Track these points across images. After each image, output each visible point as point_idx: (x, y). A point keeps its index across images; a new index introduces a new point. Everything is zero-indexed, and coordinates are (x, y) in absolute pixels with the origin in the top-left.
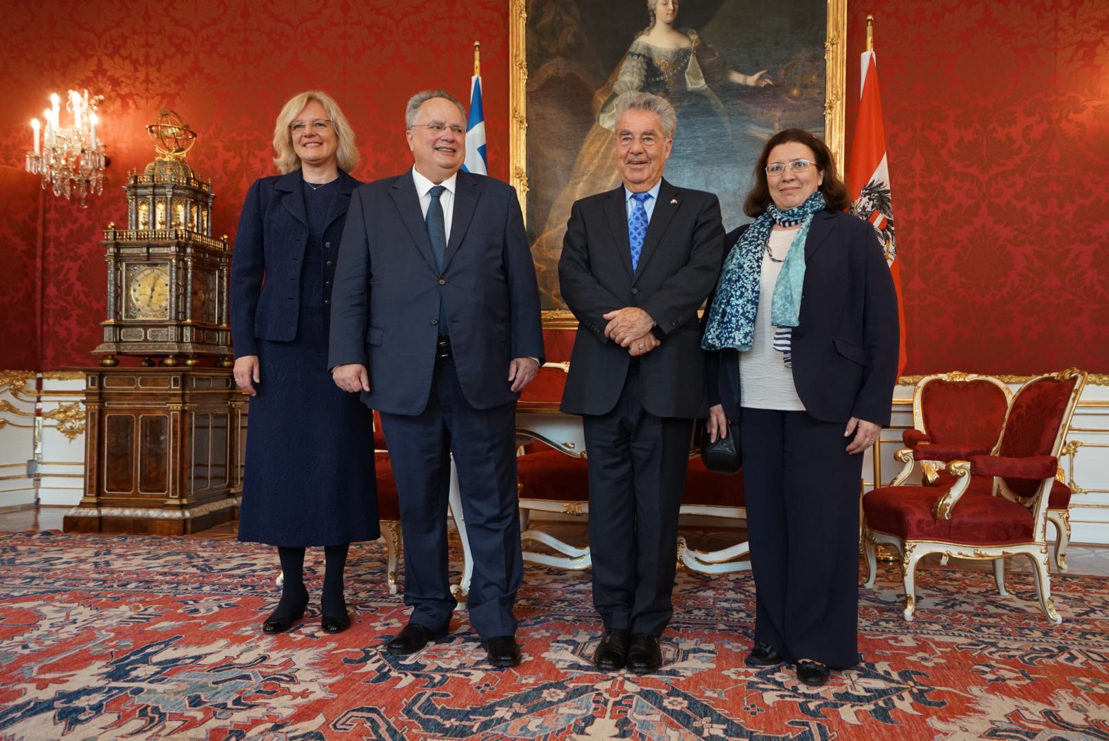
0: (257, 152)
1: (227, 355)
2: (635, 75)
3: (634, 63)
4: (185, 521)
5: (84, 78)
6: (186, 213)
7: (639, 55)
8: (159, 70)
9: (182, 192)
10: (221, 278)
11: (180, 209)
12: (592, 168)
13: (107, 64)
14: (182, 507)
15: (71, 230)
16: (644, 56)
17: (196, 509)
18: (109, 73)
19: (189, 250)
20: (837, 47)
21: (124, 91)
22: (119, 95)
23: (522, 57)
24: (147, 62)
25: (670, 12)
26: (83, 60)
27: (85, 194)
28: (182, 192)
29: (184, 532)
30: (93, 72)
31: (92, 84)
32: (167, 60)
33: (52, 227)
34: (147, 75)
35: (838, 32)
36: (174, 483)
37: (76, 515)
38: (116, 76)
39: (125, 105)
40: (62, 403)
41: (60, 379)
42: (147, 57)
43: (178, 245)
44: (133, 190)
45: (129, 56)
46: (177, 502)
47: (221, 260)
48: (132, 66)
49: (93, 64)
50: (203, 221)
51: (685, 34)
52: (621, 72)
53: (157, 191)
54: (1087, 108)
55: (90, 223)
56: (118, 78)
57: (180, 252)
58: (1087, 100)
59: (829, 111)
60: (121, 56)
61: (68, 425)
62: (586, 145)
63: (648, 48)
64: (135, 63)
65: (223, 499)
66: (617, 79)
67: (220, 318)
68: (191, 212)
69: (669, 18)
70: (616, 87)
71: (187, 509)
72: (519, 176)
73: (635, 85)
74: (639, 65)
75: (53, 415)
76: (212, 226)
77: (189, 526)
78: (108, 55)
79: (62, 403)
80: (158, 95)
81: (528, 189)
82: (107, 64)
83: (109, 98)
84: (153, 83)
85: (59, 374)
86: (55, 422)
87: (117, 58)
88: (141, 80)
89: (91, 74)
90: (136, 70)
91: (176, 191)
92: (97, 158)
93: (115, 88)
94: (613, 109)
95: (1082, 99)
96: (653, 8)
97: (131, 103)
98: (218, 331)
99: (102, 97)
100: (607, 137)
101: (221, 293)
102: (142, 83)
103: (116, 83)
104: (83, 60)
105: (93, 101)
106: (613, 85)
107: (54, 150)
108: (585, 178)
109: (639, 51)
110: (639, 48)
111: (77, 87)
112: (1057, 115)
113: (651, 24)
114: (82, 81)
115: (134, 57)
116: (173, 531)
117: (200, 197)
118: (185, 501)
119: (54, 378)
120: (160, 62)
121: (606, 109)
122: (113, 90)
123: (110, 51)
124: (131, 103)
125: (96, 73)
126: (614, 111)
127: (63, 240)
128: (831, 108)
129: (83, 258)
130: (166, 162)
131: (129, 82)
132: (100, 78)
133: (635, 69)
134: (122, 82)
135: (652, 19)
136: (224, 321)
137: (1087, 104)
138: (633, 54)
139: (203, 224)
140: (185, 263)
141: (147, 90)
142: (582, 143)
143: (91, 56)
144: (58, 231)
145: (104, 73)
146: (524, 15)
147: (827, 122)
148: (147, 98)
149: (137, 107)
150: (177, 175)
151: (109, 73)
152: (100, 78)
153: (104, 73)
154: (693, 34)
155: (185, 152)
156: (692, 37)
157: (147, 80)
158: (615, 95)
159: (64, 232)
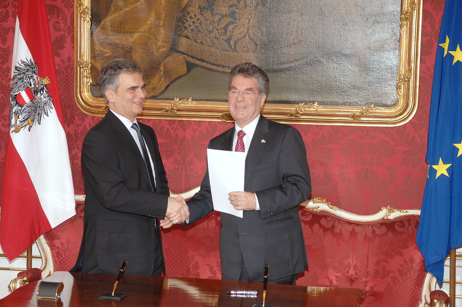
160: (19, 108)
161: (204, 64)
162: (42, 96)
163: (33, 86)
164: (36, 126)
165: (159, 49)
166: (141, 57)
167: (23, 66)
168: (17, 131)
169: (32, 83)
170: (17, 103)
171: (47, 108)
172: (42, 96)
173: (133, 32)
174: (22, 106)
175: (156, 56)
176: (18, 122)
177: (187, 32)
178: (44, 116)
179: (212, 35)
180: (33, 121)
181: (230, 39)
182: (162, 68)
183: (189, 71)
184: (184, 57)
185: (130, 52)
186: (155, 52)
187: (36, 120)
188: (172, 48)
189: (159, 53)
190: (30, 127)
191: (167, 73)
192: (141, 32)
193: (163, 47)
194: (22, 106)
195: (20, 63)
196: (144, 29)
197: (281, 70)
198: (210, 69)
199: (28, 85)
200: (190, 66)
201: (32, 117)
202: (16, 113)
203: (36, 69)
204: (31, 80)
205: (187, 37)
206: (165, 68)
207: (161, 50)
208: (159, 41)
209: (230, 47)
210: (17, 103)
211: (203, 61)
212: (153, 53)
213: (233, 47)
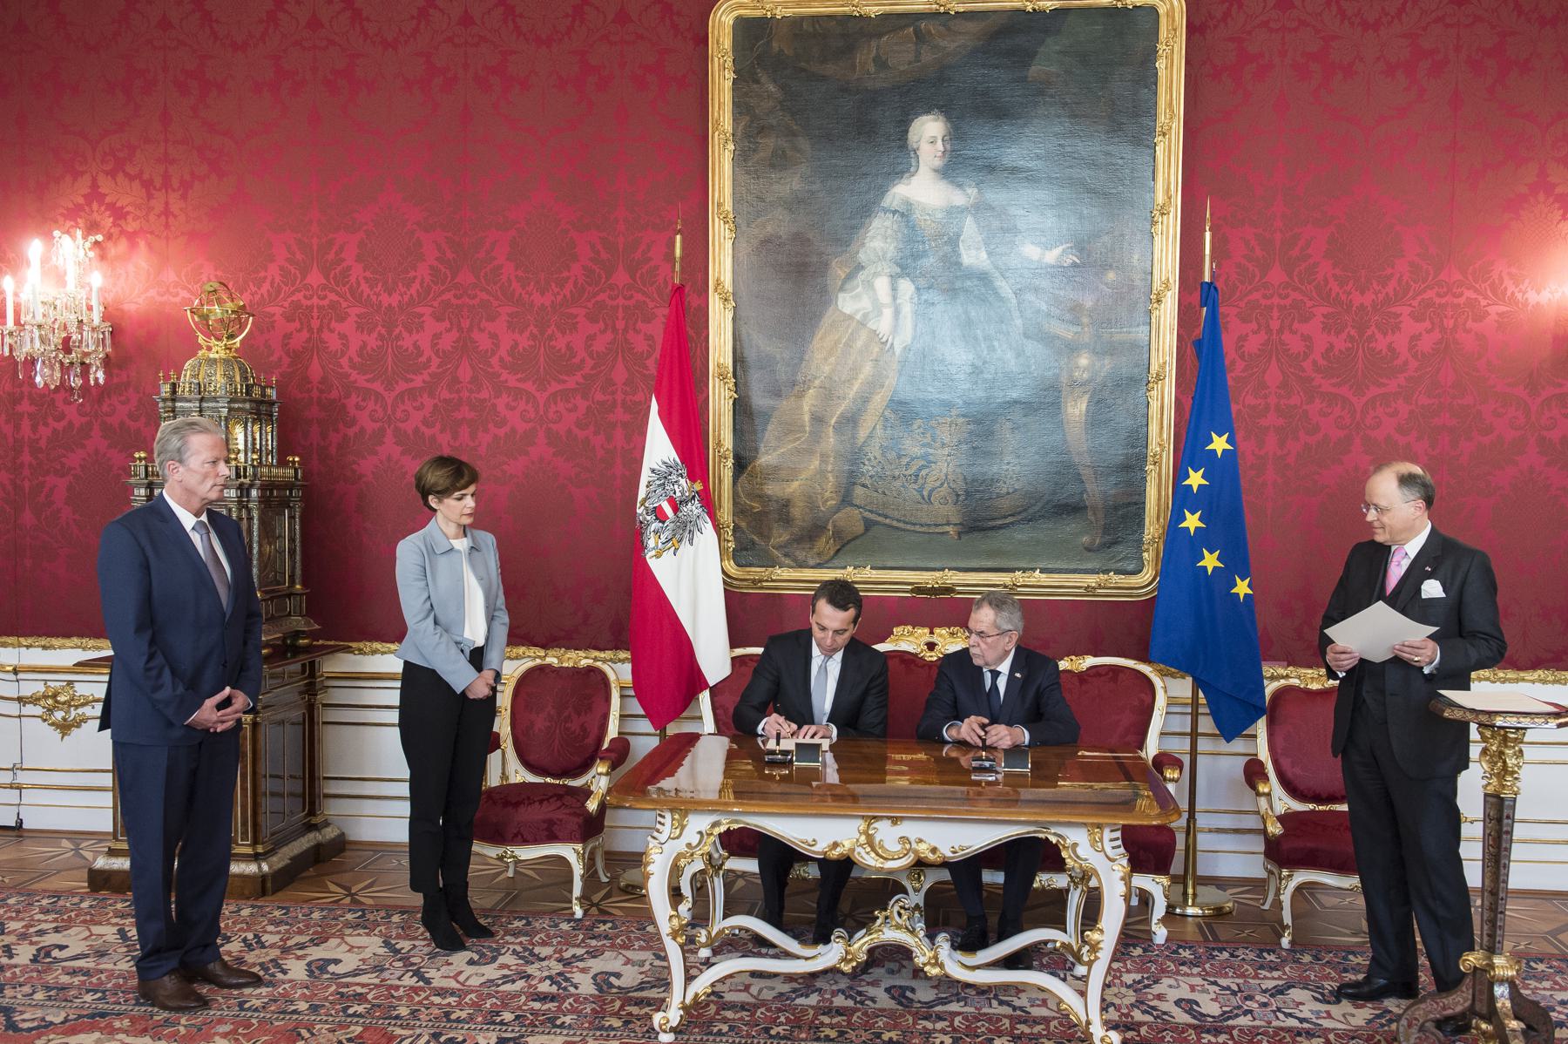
0: (333, 324)
1: (303, 632)
2: (889, 240)
3: (888, 223)
4: (264, 877)
5: (71, 205)
6: (246, 436)
7: (895, 212)
8: (184, 197)
9: (241, 405)
10: (292, 517)
11: (239, 433)
12: (827, 369)
13: (105, 185)
14: (256, 857)
15: (55, 431)
16: (903, 215)
17: (275, 859)
18: (108, 200)
19: (254, 493)
20: (1168, 218)
21: (131, 225)
22: (123, 232)
23: (728, 206)
24: (166, 185)
25: (940, 154)
26: (68, 178)
27: (79, 382)
28: (241, 405)
29: (264, 893)
30: (85, 196)
31: (82, 214)
32: (196, 183)
33: (26, 424)
34: (167, 204)
35: (1170, 198)
36: (244, 824)
37: (107, 867)
38: (119, 204)
39: (133, 245)
40: (49, 683)
41: (44, 647)
42: (166, 178)
43: (240, 487)
44: (169, 404)
45: (139, 176)
46: (249, 851)
47: (291, 493)
48: (144, 190)
49: (83, 185)
50: (267, 440)
51: (960, 186)
52: (869, 234)
53: (205, 405)
54: (1489, 314)
55: (84, 420)
56: (122, 208)
57: (242, 496)
58: (1489, 305)
59: (1155, 305)
60: (127, 175)
61: (59, 715)
62: (819, 334)
63: (908, 204)
64: (148, 185)
65: (303, 836)
66: (863, 244)
67: (292, 577)
68: (252, 432)
69: (938, 163)
70: (862, 257)
71: (264, 860)
72: (722, 377)
73: (889, 255)
74: (895, 227)
75: (39, 699)
76: (278, 445)
77: (269, 885)
78: (107, 173)
79: (49, 683)
80: (182, 233)
81: (736, 396)
82: (105, 185)
83: (109, 237)
84: (175, 216)
85: (44, 641)
86: (38, 710)
87: (120, 177)
88: (157, 211)
89: (81, 201)
90: (150, 196)
91: (232, 405)
92: (101, 336)
93: (120, 222)
94: (858, 286)
95: (1484, 302)
96: (915, 146)
97: (142, 244)
98: (289, 596)
99: (100, 238)
100: (848, 327)
101: (292, 540)
102: (159, 216)
103: (119, 214)
104: (68, 178)
105: (88, 245)
106: (858, 252)
107: (40, 326)
108: (817, 382)
109: (895, 205)
110: (895, 203)
111: (61, 219)
112: (1452, 322)
113: (912, 169)
114: (68, 209)
115: (146, 176)
116: (246, 892)
117: (263, 408)
118: (260, 849)
119: (38, 646)
120: (186, 186)
121: (847, 286)
122: (115, 224)
123: (109, 167)
124: (142, 244)
125: (89, 198)
126: (860, 289)
127: (43, 444)
128: (1159, 301)
129: (72, 472)
130: (215, 360)
131: (138, 212)
132: (95, 206)
133: (889, 232)
134: (128, 213)
135: (913, 162)
136: (297, 581)
137: (1488, 309)
138: (886, 211)
139: (267, 445)
140: (249, 511)
141: (167, 226)
142: (813, 334)
143: (82, 173)
144: (34, 428)
145: (101, 198)
146: (731, 147)
147: (1153, 320)
148: (167, 238)
149: (150, 246)
150: (231, 379)
151: (108, 200)
152: (95, 206)
153: (101, 198)
154: (970, 186)
155: (238, 339)
156: (969, 191)
157: (167, 212)
158: (860, 267)
159: (45, 432)
160: (661, 525)
161: (888, 521)
162: (694, 508)
163: (678, 494)
164: (685, 548)
165: (827, 501)
167: (664, 468)
168: (658, 556)
169: (677, 490)
170: (657, 519)
171: (700, 522)
172: (694, 508)
174: (663, 523)
176: (660, 544)
178: (697, 533)
179: (898, 484)
180: (680, 541)
181: (922, 488)
182: (830, 527)
183: (867, 529)
184: (861, 513)
185: (787, 506)
187: (686, 540)
188: (843, 501)
190: (676, 550)
191: (837, 534)
193: (833, 499)
194: (663, 523)
195: (660, 464)
197: (992, 528)
198: (897, 528)
199: (672, 494)
200: (869, 525)
201: (678, 536)
202: (656, 532)
203: (684, 472)
204: (676, 486)
205: (864, 486)
206: (835, 526)
209: (924, 499)
210: (657, 519)
211: (886, 517)
213: (926, 497)
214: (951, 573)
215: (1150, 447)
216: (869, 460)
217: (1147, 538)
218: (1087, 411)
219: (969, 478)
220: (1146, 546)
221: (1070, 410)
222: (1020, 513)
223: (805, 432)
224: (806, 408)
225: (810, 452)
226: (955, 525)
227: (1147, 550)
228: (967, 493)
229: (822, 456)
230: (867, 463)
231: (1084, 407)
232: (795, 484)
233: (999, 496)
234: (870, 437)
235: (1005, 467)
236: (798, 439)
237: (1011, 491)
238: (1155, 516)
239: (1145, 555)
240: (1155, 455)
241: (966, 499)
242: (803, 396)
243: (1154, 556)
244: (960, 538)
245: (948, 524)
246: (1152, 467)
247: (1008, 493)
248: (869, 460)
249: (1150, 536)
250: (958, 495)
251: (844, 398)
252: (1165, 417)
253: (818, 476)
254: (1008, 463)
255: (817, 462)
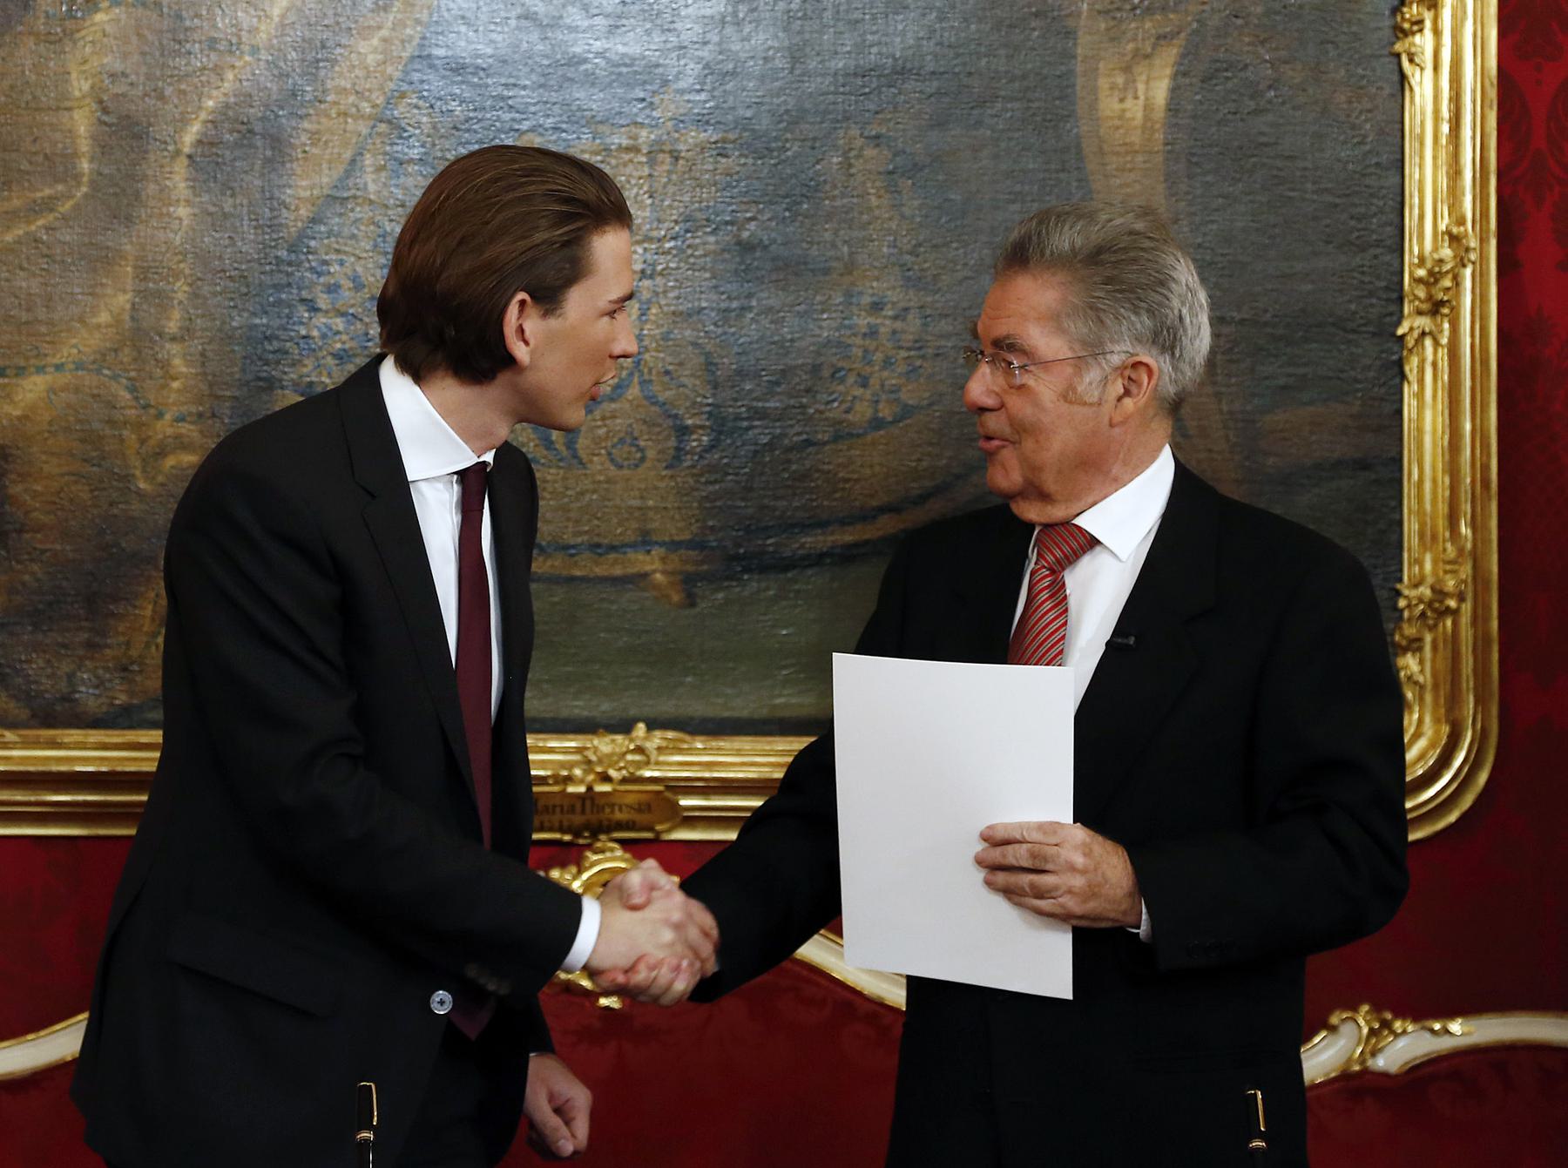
165: (161, 453)
166: (57, 500)
173: (14, 372)
175: (140, 494)
177: (310, 367)
186: (138, 473)
189: (160, 479)
192: (59, 367)
196: (75, 351)
207: (170, 462)
208: (160, 416)
212: (127, 478)
214: (658, 738)
215: (1412, 250)
216: (332, 289)
217: (1413, 594)
218: (1173, 108)
219: (728, 363)
220: (1410, 630)
221: (1109, 105)
222: (923, 498)
223: (77, 177)
224: (80, 86)
225: (101, 260)
226: (674, 546)
227: (1415, 645)
228: (721, 425)
229: (144, 272)
230: (323, 301)
231: (1160, 91)
232: (33, 388)
233: (843, 434)
234: (336, 199)
235: (863, 321)
236: (48, 205)
237: (886, 412)
238: (1443, 508)
239: (1409, 664)
240: (1434, 277)
241: (711, 448)
242: (69, 34)
243: (1442, 665)
244: (691, 601)
245: (645, 541)
246: (1424, 322)
247: (877, 423)
248: (332, 289)
249: (1425, 591)
250: (683, 431)
251: (233, 48)
252: (1466, 132)
253: (126, 355)
254: (876, 307)
255: (123, 300)
